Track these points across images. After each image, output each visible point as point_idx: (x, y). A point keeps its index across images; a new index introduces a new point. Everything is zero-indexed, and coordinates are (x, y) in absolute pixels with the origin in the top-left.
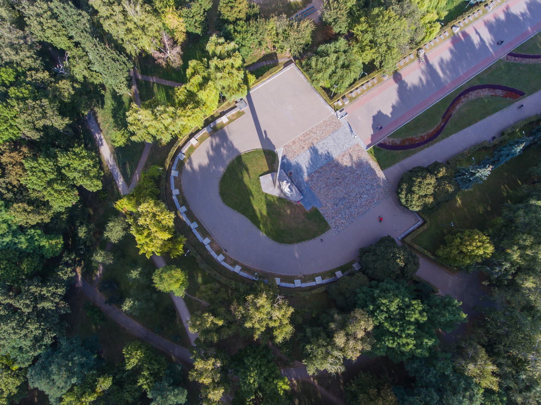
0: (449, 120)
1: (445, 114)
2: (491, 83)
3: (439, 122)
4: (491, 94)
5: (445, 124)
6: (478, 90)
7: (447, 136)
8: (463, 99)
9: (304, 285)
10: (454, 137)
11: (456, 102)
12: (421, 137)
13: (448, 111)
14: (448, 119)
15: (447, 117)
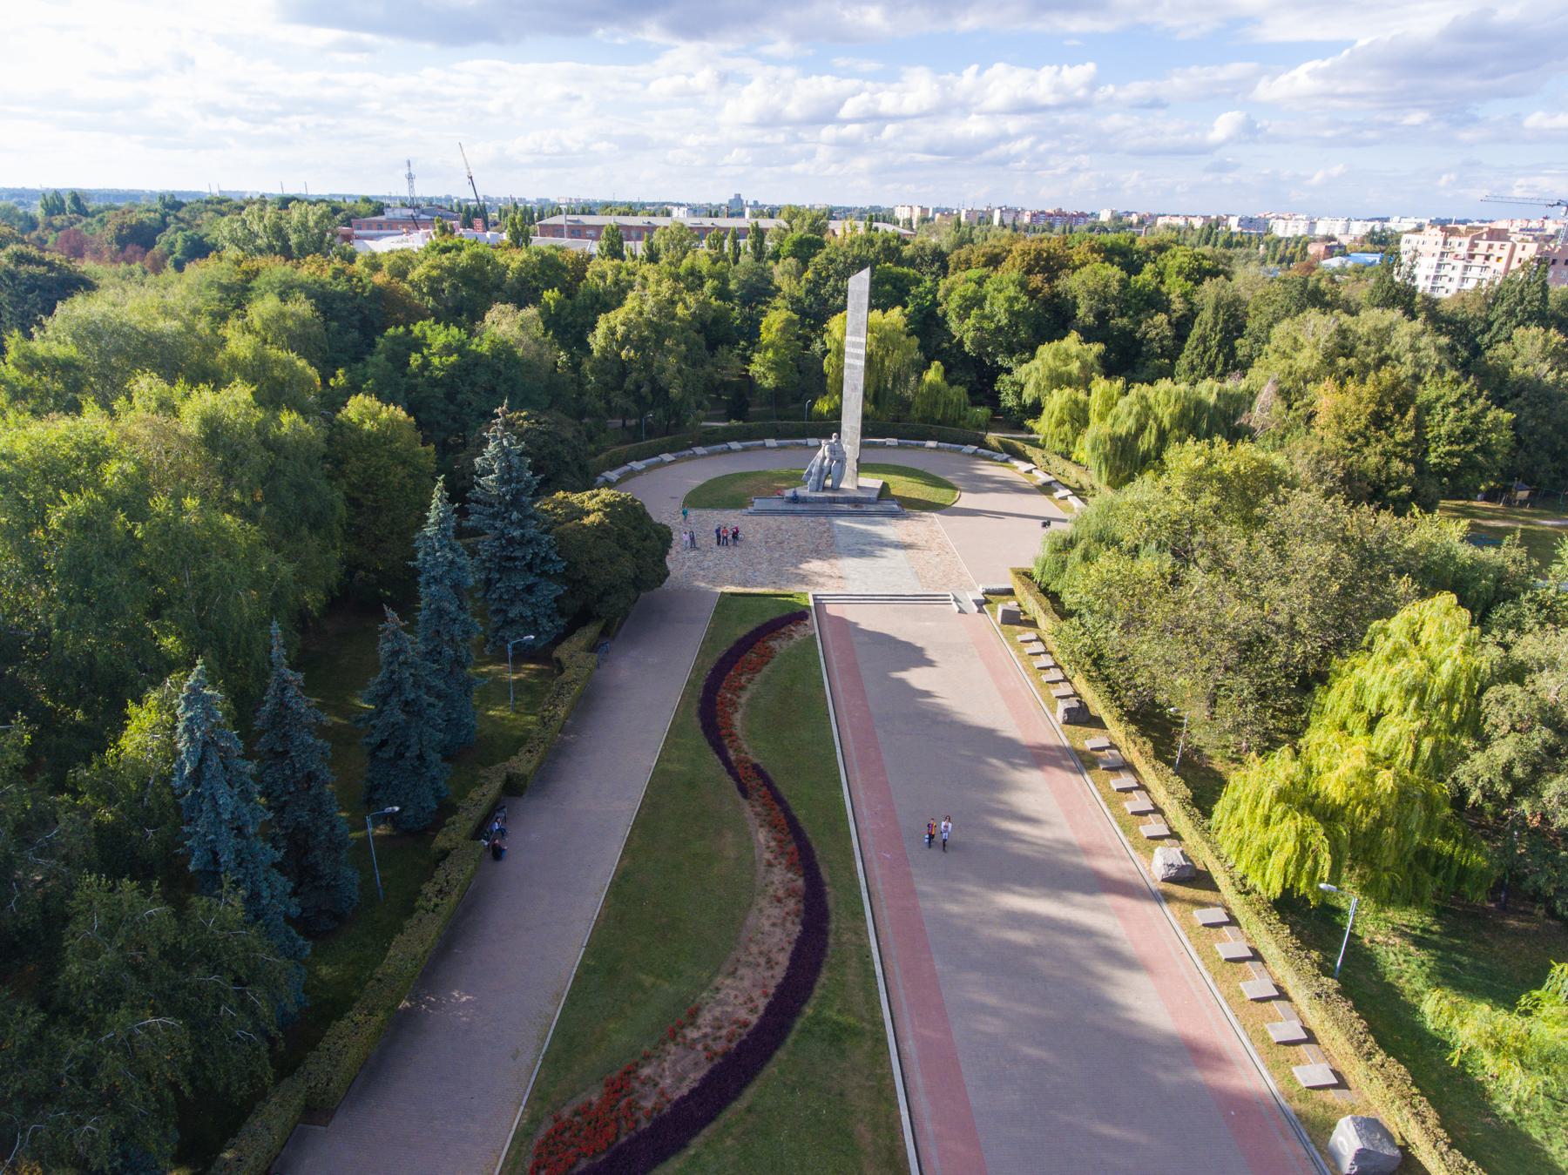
0: (729, 781)
1: (768, 783)
2: (771, 1069)
3: (750, 746)
4: (706, 1018)
5: (727, 762)
6: (780, 973)
7: (676, 730)
8: (782, 877)
9: (626, 468)
10: (649, 761)
11: (792, 847)
12: (742, 688)
13: (777, 799)
14: (737, 779)
15: (753, 781)
